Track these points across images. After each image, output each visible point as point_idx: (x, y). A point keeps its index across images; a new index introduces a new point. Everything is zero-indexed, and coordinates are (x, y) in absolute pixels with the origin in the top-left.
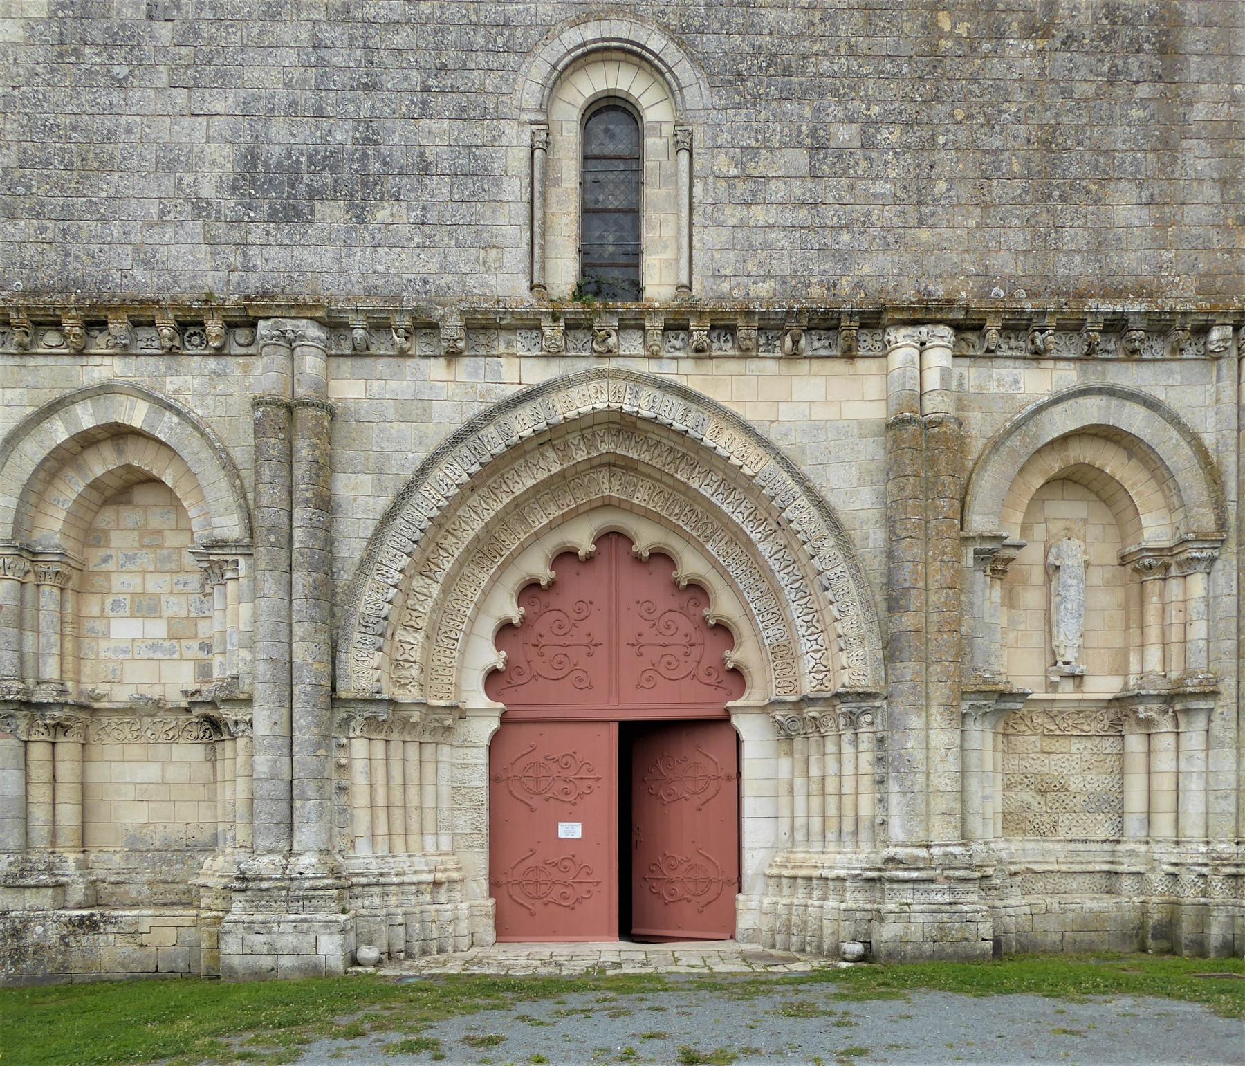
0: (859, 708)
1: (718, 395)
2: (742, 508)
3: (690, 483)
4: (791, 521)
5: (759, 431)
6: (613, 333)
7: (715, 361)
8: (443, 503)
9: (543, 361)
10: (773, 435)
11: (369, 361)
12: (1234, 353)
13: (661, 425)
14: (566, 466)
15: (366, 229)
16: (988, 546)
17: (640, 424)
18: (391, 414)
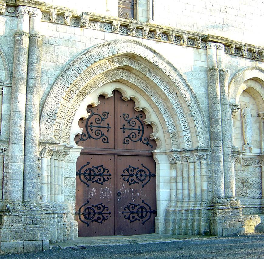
0: (203, 154)
16: (233, 107)
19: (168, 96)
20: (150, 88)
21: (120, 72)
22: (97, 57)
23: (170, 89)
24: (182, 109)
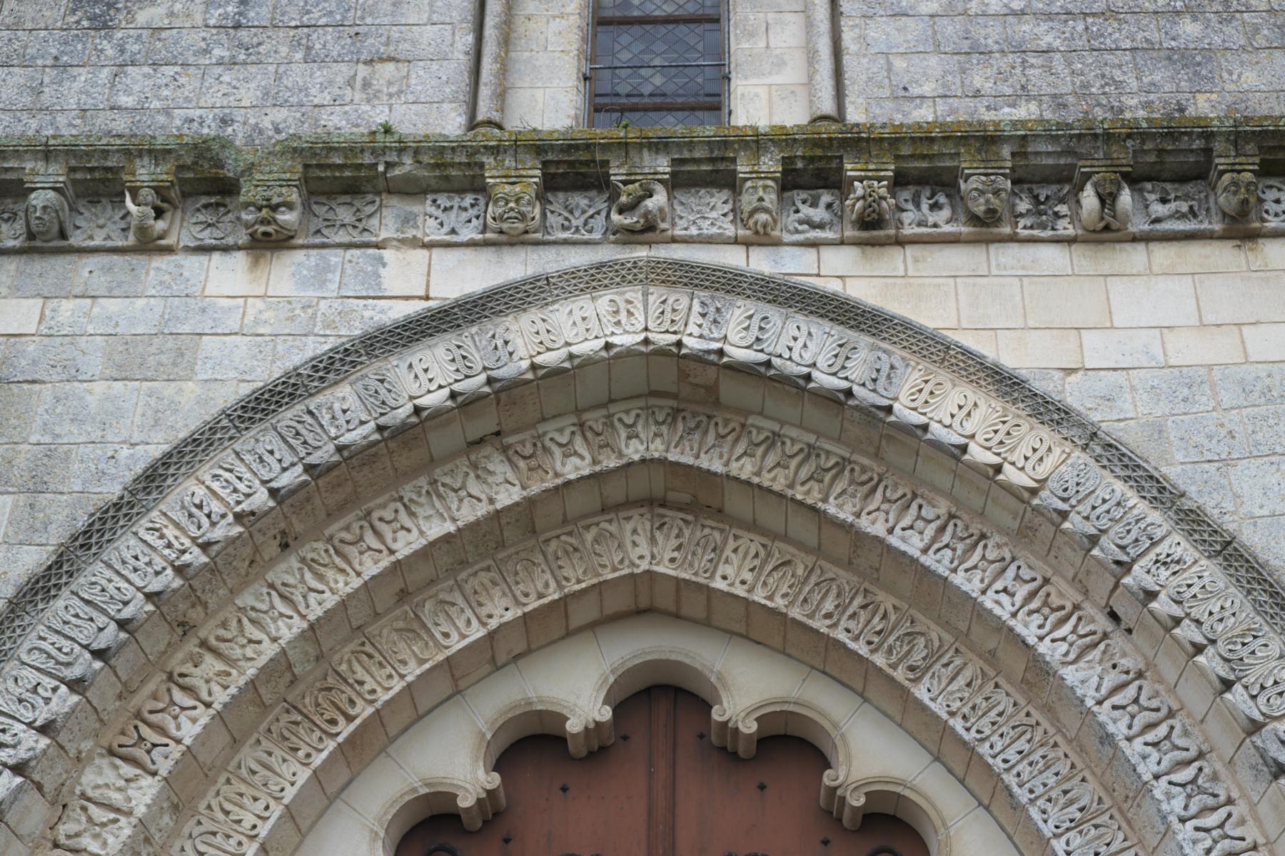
1: (930, 315)
2: (1008, 579)
3: (864, 523)
4: (1151, 595)
5: (1038, 386)
6: (659, 188)
7: (910, 250)
8: (196, 557)
9: (487, 255)
10: (1074, 394)
11: (59, 264)
13: (784, 380)
14: (535, 489)
15: (109, 38)
17: (730, 390)
18: (94, 363)
19: (1032, 640)
20: (893, 618)
21: (629, 527)
22: (364, 417)
23: (1046, 581)
24: (1186, 733)
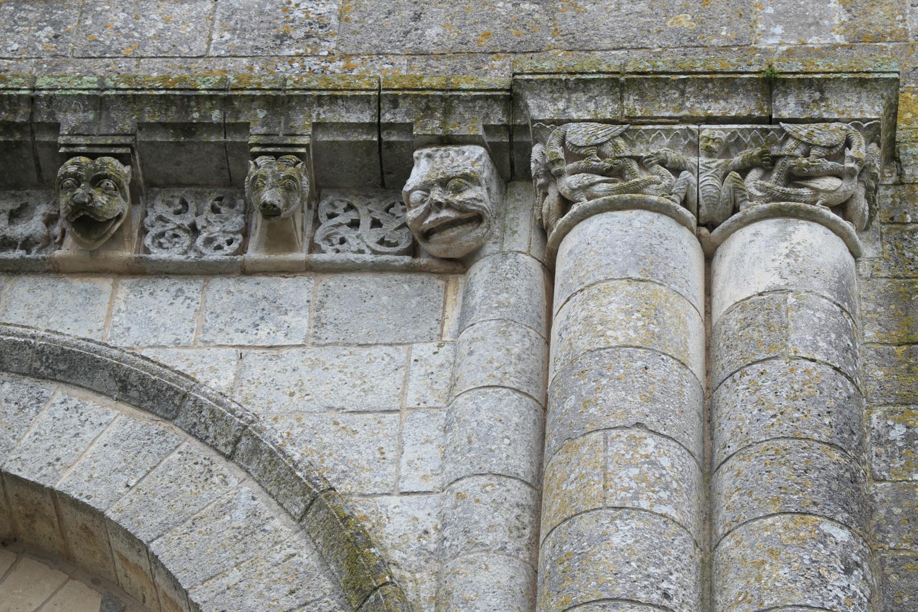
12: (522, 236)
